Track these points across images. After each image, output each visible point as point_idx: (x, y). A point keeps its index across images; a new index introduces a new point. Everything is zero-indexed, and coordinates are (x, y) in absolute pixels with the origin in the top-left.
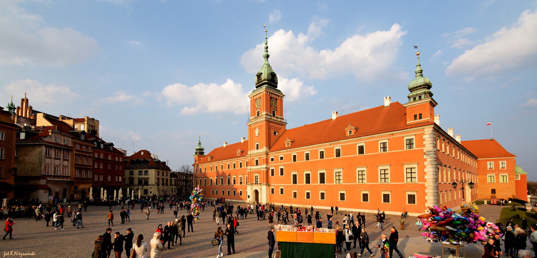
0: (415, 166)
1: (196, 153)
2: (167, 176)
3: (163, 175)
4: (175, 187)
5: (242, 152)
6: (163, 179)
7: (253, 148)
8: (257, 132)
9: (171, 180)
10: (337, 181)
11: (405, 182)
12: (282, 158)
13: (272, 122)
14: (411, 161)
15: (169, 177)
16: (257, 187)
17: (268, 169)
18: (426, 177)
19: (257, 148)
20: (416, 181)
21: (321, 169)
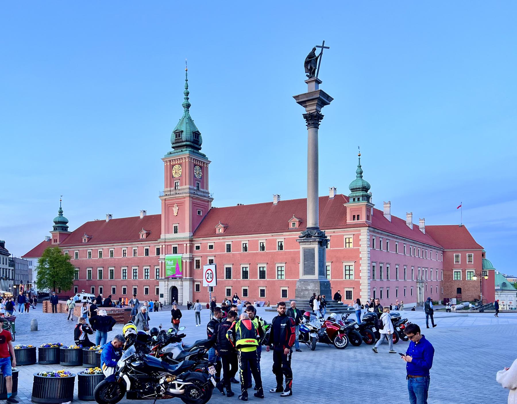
0: (353, 264)
1: (55, 229)
2: (6, 264)
3: (3, 264)
4: (12, 282)
5: (148, 234)
6: (3, 269)
7: (168, 231)
8: (175, 210)
9: (9, 270)
10: (280, 277)
11: (344, 279)
12: (211, 247)
13: (197, 199)
14: (349, 259)
15: (7, 267)
16: (177, 284)
17: (192, 259)
18: (361, 275)
19: (176, 232)
20: (352, 277)
21: (260, 263)
